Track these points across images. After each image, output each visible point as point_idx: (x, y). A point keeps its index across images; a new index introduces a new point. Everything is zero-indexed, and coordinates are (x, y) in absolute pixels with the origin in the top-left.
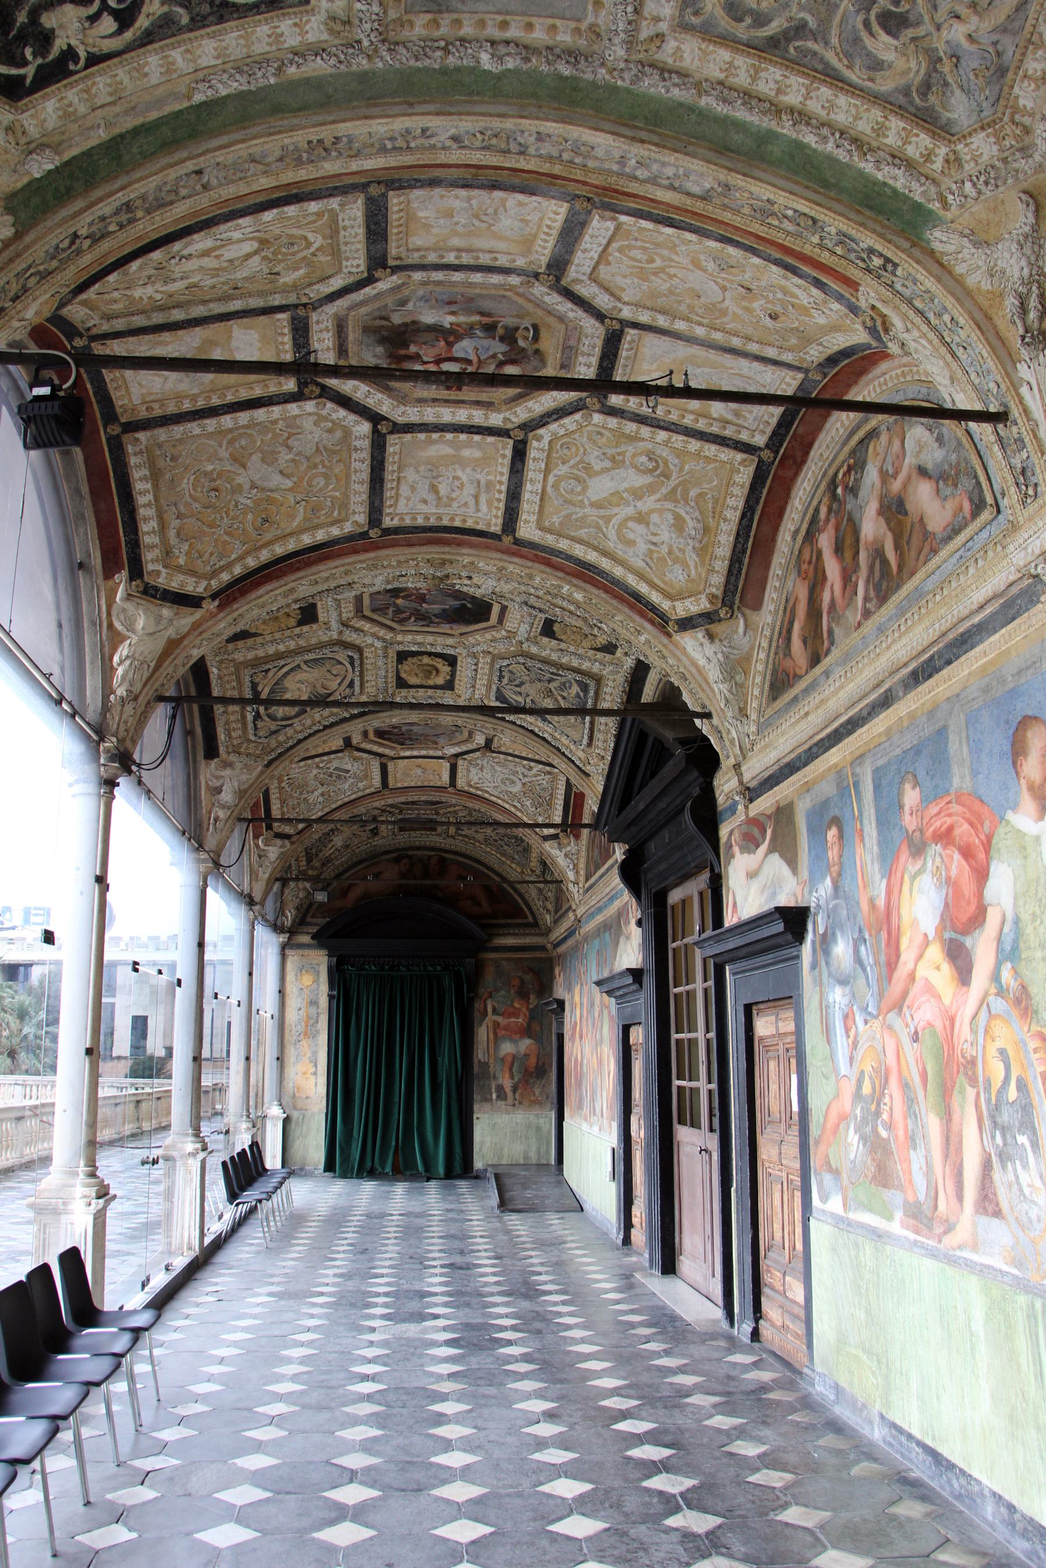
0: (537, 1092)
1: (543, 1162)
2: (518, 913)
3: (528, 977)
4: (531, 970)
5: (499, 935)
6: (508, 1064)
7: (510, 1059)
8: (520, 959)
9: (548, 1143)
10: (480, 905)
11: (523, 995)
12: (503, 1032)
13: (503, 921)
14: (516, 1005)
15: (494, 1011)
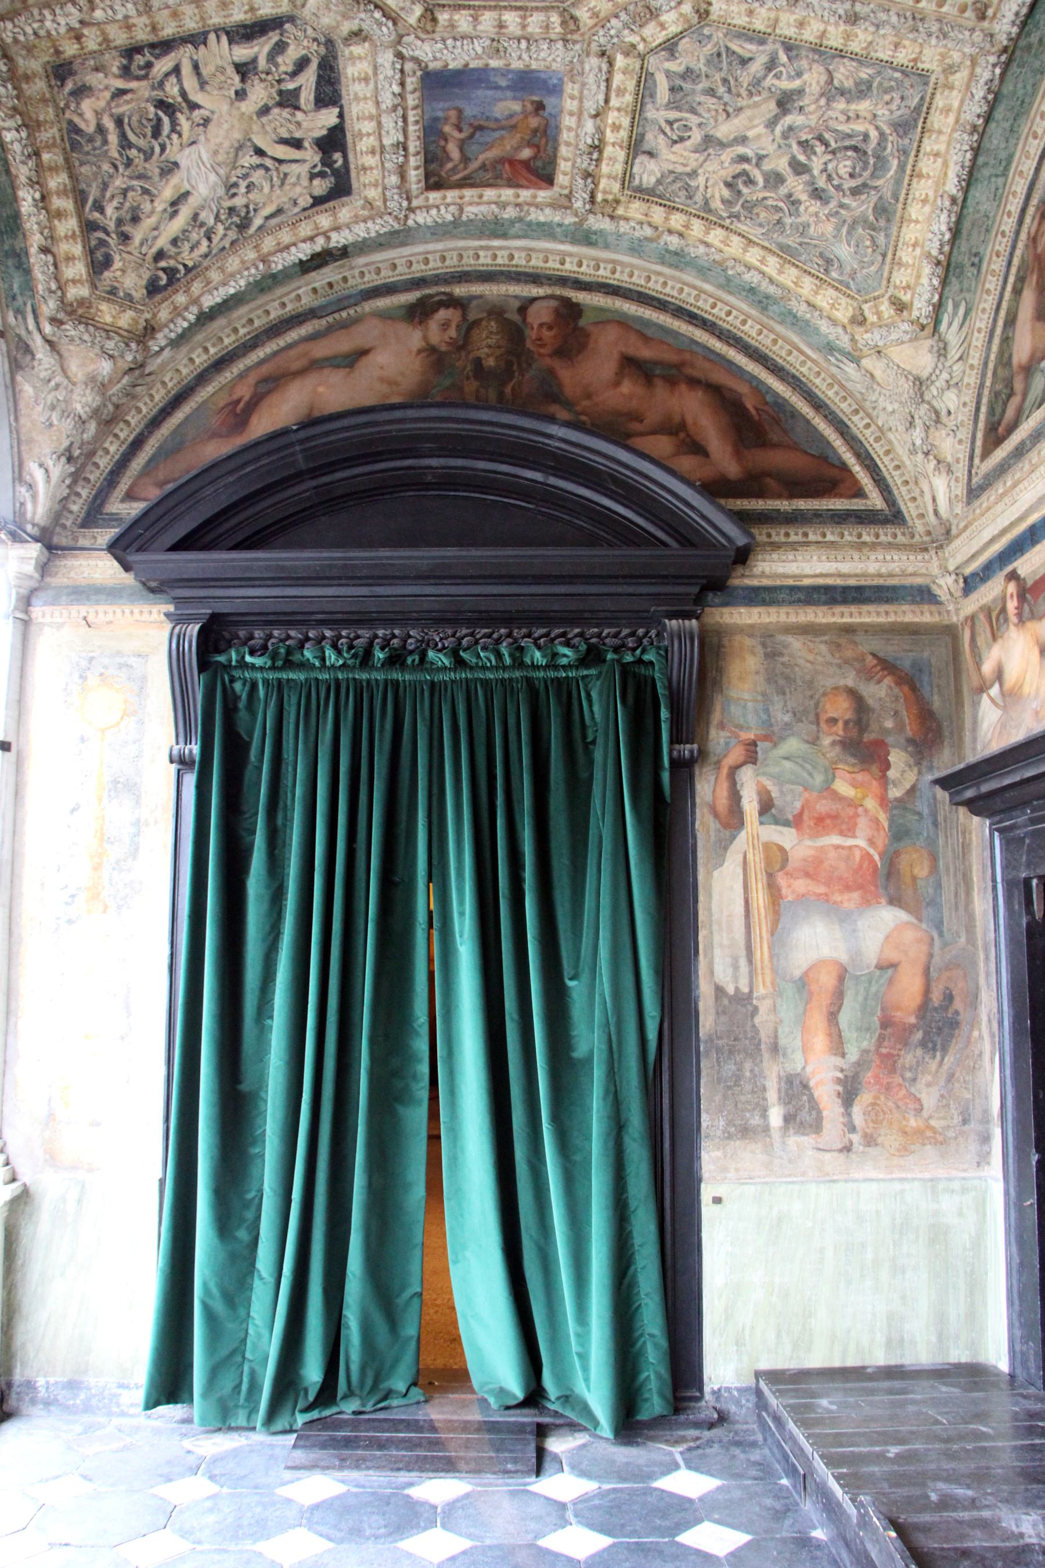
0: (929, 1098)
1: (958, 1355)
2: (825, 478)
3: (879, 692)
4: (887, 666)
5: (776, 546)
6: (822, 1001)
7: (827, 980)
8: (849, 630)
9: (975, 1286)
10: (697, 449)
11: (865, 750)
12: (801, 885)
13: (784, 505)
14: (843, 787)
15: (766, 806)
